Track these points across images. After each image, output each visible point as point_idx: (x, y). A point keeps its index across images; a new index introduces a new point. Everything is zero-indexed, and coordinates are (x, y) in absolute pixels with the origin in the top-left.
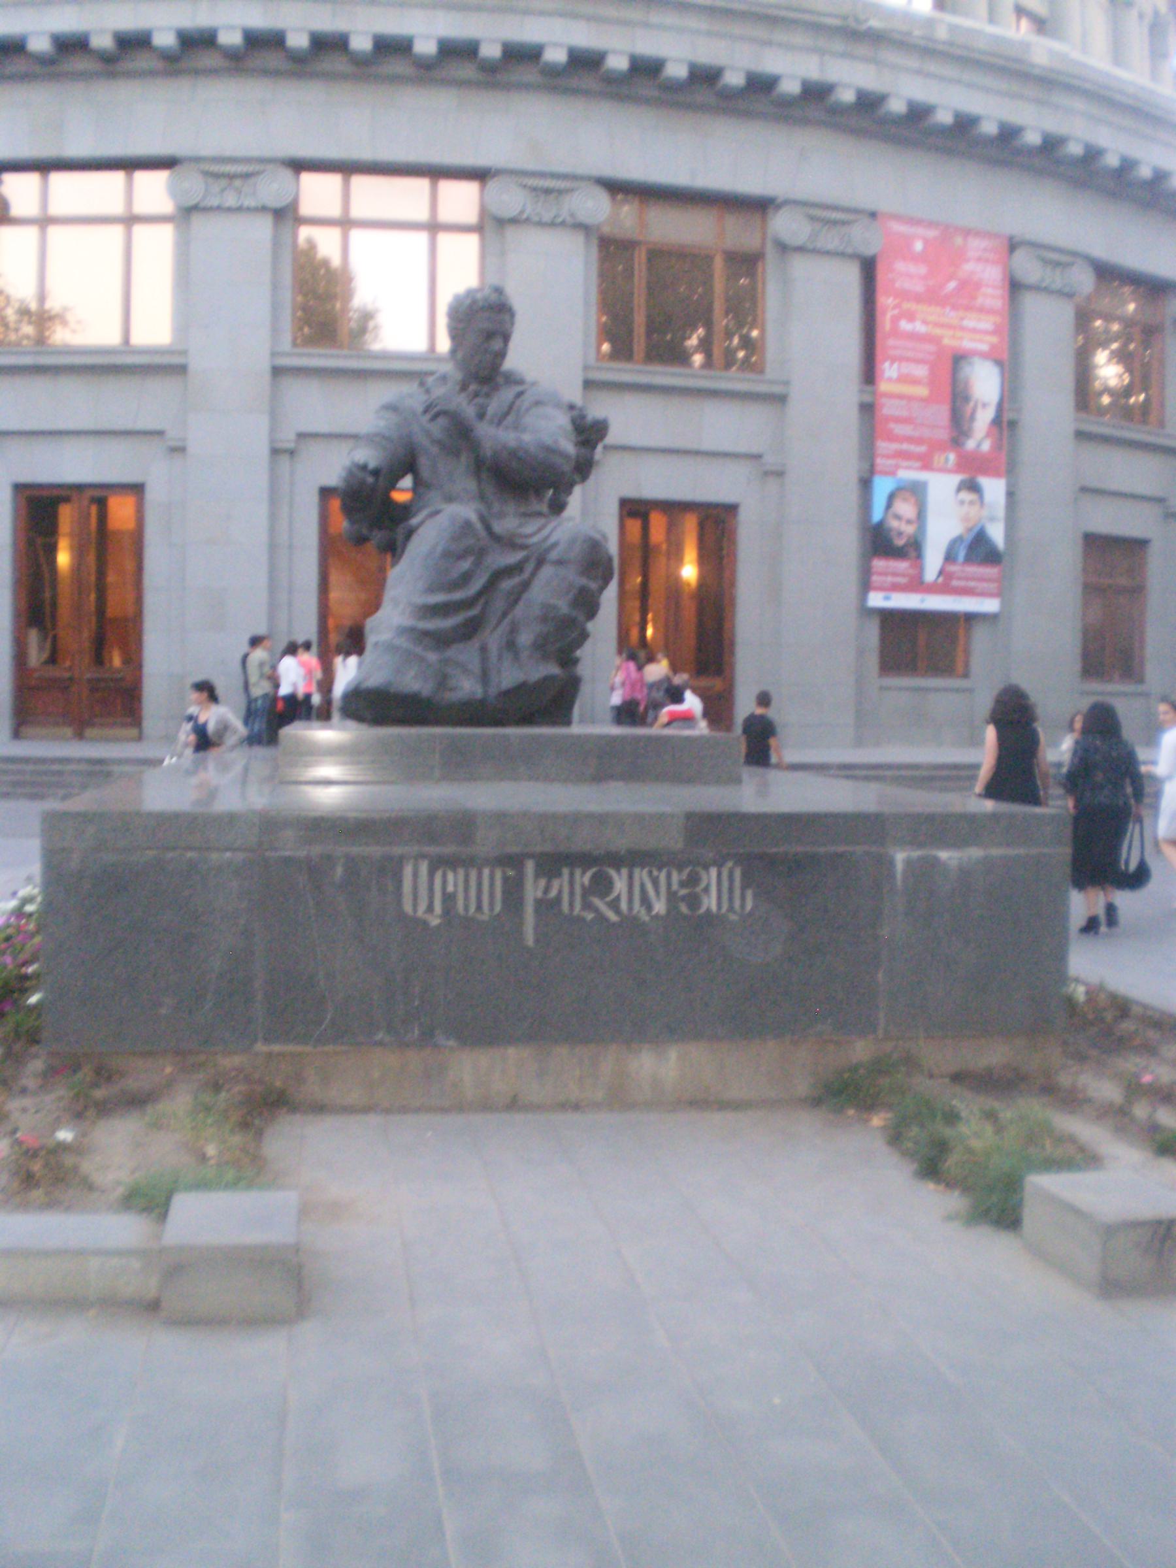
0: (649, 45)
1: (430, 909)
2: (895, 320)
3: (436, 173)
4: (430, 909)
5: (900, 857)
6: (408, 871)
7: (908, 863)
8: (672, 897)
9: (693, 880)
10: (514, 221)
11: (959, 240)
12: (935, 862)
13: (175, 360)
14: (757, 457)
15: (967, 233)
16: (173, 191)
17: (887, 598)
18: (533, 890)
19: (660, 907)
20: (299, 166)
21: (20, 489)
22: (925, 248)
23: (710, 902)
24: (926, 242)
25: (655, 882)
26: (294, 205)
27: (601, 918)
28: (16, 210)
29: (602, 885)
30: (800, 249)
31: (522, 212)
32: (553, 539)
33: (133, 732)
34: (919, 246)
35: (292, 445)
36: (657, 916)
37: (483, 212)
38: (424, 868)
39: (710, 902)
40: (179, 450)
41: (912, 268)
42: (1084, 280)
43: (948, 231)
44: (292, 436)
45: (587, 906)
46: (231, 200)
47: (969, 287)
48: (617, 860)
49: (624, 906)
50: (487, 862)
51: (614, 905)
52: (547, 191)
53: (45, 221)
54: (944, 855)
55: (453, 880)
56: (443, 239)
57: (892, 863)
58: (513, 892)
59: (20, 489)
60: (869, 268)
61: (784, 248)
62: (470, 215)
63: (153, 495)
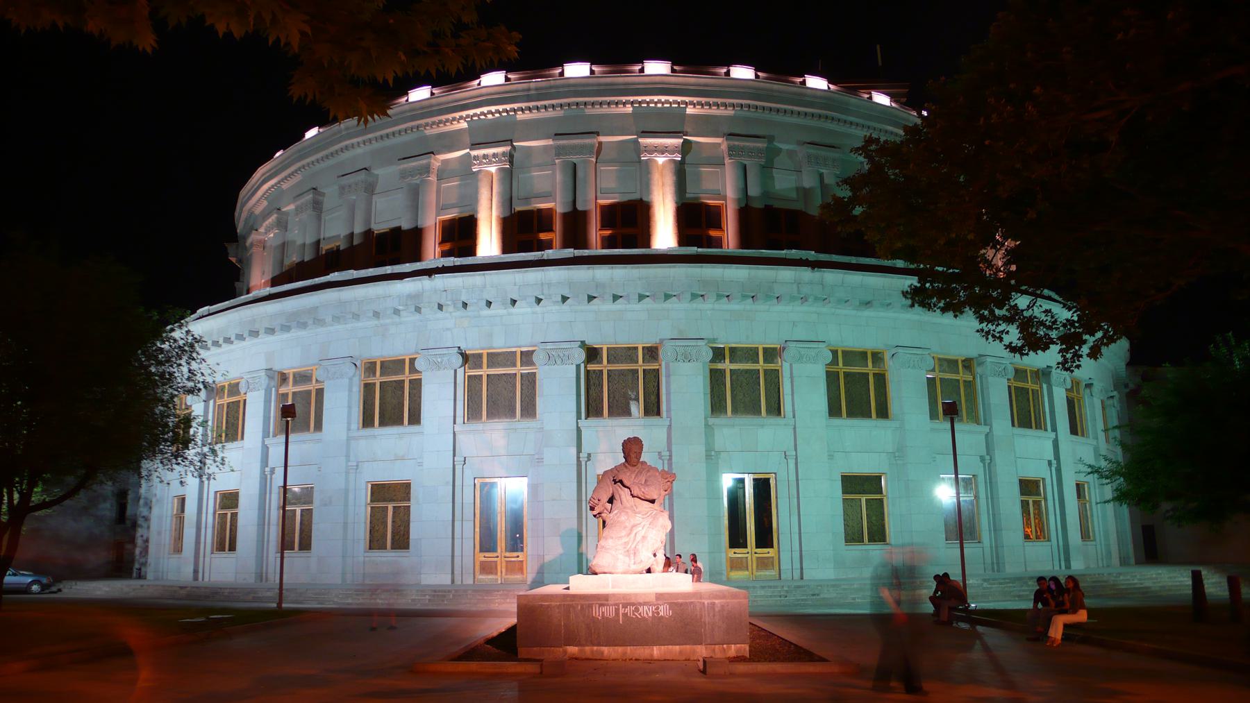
1: (599, 615)
4: (599, 615)
7: (708, 603)
8: (653, 612)
9: (658, 608)
12: (714, 604)
18: (621, 611)
19: (650, 614)
23: (661, 614)
25: (649, 610)
27: (638, 617)
29: (637, 610)
36: (650, 617)
38: (597, 605)
39: (661, 614)
45: (634, 614)
48: (640, 604)
50: (612, 605)
51: (640, 614)
58: (617, 611)
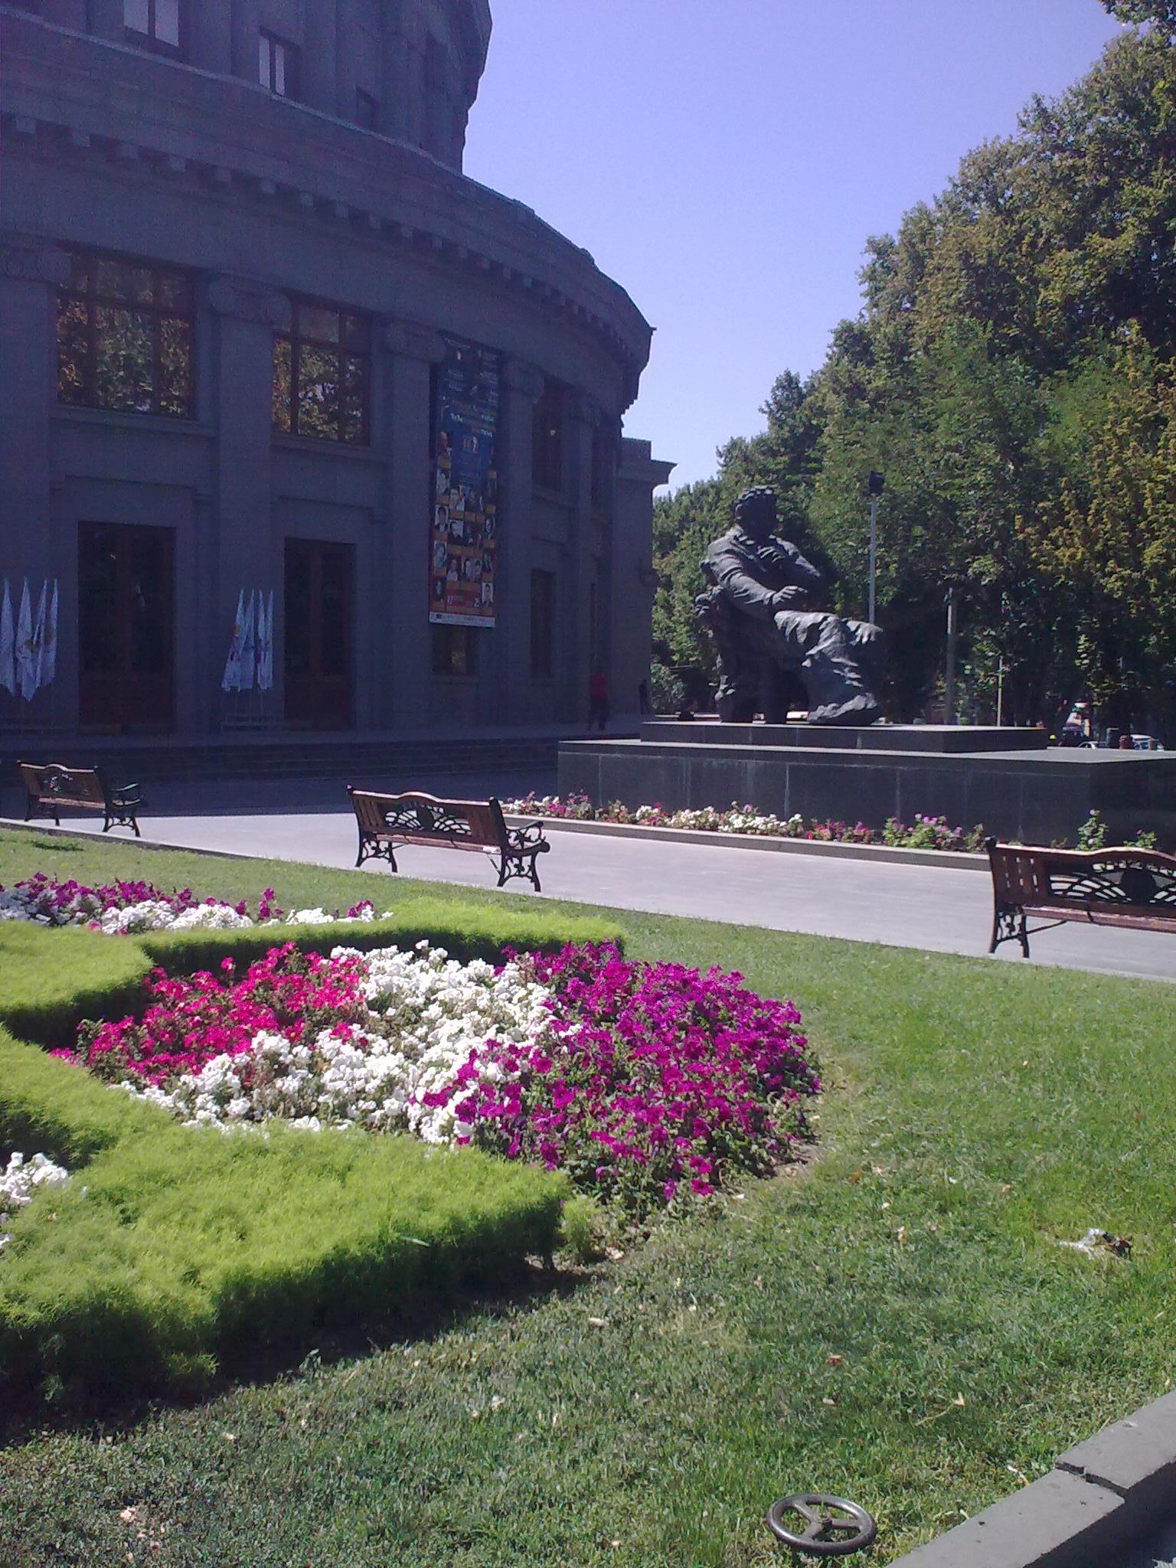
2: (447, 412)
47: (484, 389)
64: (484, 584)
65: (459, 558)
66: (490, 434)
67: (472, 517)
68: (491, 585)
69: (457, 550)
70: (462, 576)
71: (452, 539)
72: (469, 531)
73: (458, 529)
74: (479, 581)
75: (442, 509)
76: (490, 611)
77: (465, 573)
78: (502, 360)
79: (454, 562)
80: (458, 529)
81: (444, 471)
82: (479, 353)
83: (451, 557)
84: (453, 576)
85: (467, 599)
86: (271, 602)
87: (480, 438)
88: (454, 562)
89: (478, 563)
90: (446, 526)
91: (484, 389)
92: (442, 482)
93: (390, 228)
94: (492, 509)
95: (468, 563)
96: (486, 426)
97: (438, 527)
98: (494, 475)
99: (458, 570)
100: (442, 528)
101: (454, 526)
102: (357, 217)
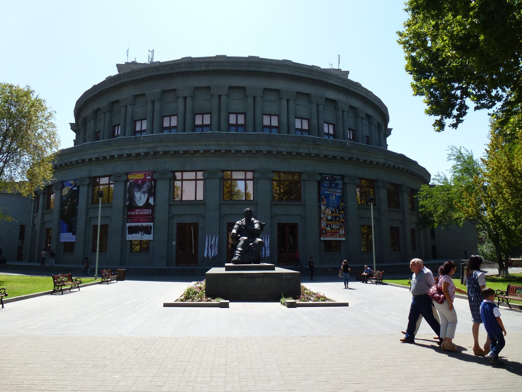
0: (280, 149)
2: (324, 191)
3: (246, 171)
5: (284, 277)
6: (238, 278)
10: (259, 178)
11: (335, 177)
13: (205, 203)
14: (301, 215)
15: (336, 175)
16: (203, 175)
17: (324, 238)
19: (261, 282)
20: (223, 171)
21: (177, 223)
22: (328, 178)
24: (329, 177)
26: (223, 177)
28: (177, 179)
30: (306, 180)
31: (260, 177)
32: (256, 241)
33: (196, 264)
34: (327, 178)
35: (223, 216)
37: (253, 177)
40: (204, 217)
41: (326, 182)
42: (358, 181)
43: (333, 175)
44: (223, 215)
46: (213, 177)
48: (257, 277)
49: (258, 281)
52: (264, 174)
53: (182, 180)
54: (288, 276)
55: (242, 279)
56: (247, 182)
57: (283, 277)
59: (177, 223)
60: (319, 183)
61: (304, 181)
62: (252, 178)
63: (200, 225)
64: (340, 230)
65: (330, 225)
66: (340, 195)
67: (334, 215)
68: (343, 230)
69: (330, 223)
70: (332, 229)
71: (327, 220)
72: (333, 218)
73: (329, 217)
74: (339, 229)
75: (324, 213)
76: (344, 236)
77: (332, 228)
78: (343, 177)
79: (329, 226)
80: (329, 217)
81: (324, 205)
82: (335, 177)
83: (327, 225)
84: (328, 229)
85: (334, 233)
86: (269, 238)
87: (336, 196)
88: (329, 226)
89: (337, 225)
90: (325, 217)
91: (337, 185)
92: (323, 207)
93: (299, 154)
94: (343, 212)
95: (333, 225)
96: (338, 193)
97: (323, 218)
98: (343, 204)
99: (330, 227)
100: (324, 218)
101: (328, 217)
102: (289, 153)
